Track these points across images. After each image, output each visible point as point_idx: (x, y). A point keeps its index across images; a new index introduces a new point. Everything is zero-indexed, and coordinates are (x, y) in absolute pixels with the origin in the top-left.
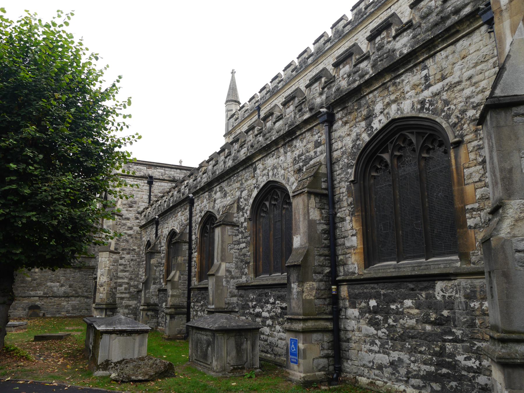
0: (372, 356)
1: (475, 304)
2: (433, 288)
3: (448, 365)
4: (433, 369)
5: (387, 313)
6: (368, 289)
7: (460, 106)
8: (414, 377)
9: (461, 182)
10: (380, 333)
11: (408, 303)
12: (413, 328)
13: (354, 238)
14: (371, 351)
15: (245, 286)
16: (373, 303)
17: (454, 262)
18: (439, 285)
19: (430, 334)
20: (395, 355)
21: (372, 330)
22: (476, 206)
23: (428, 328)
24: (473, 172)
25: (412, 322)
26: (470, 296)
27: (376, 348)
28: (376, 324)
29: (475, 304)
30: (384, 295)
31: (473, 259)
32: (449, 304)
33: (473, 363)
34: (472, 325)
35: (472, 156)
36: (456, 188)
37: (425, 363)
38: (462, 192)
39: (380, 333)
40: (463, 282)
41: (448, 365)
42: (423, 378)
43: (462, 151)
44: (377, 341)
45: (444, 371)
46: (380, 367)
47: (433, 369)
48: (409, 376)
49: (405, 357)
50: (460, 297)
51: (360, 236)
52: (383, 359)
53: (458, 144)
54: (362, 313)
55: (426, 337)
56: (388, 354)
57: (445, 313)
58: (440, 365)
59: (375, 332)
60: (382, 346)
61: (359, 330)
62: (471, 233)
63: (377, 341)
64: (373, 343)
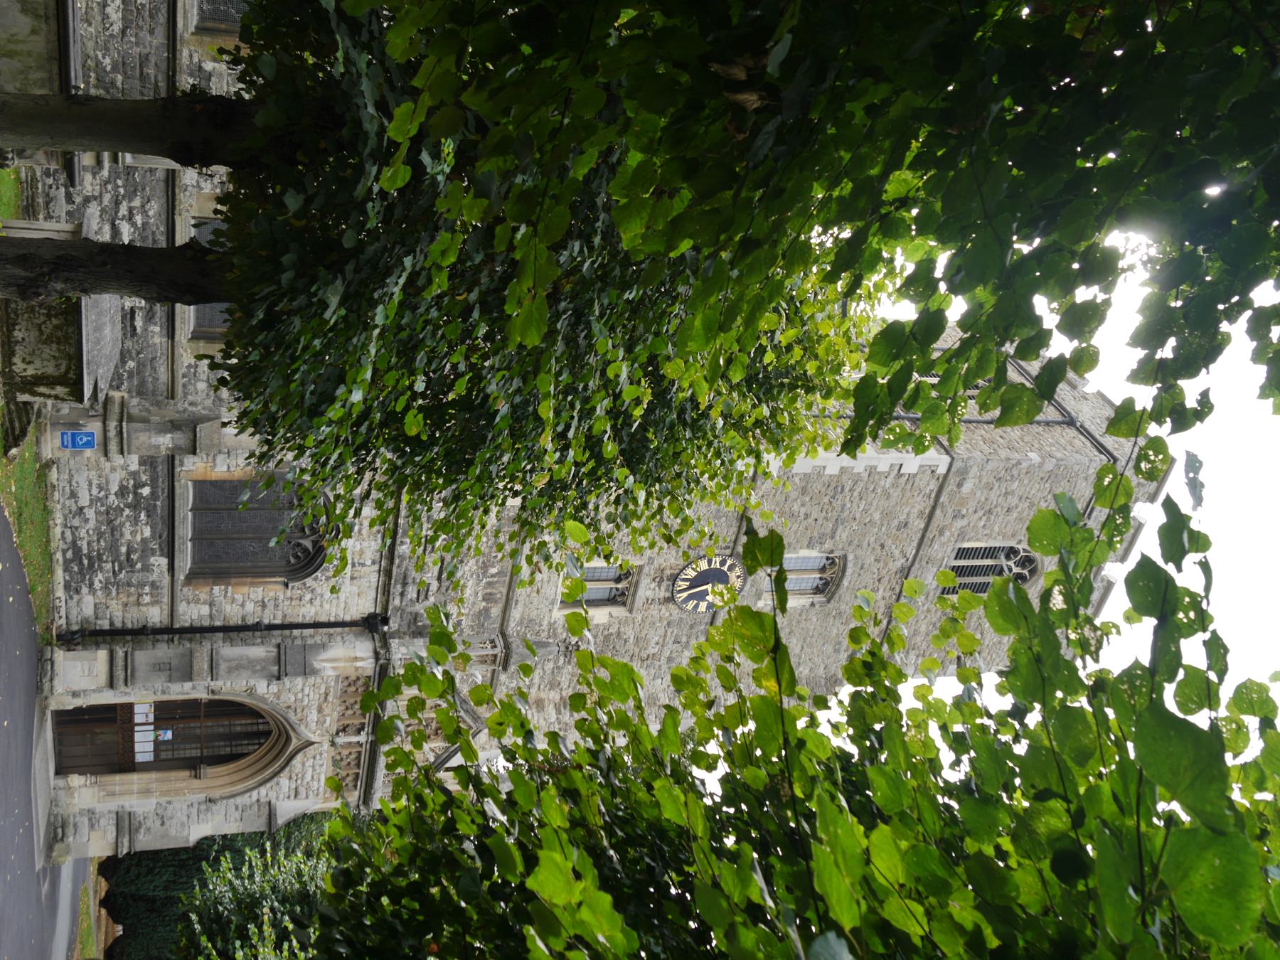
0: (85, 485)
1: (147, 589)
2: (161, 555)
3: (91, 565)
4: (85, 551)
5: (135, 506)
6: (162, 483)
7: (319, 590)
8: (73, 533)
9: (252, 584)
10: (112, 498)
11: (147, 532)
12: (122, 535)
13: (225, 468)
14: (90, 485)
15: (174, 208)
16: (146, 491)
17: (185, 561)
18: (164, 561)
19: (117, 550)
20: (90, 514)
21: (114, 488)
22: (229, 594)
23: (124, 549)
24: (258, 592)
25: (128, 536)
26: (153, 585)
27: (95, 491)
28: (122, 492)
29: (147, 589)
30: (155, 506)
31: (185, 589)
32: (147, 568)
33: (97, 585)
34: (129, 585)
35: (272, 594)
36: (249, 580)
37: (89, 544)
38: (244, 584)
39: (112, 498)
40: (166, 580)
41: (91, 565)
42: (74, 542)
43: (281, 587)
44: (103, 493)
45: (86, 562)
46: (73, 495)
47: (85, 551)
48: (74, 529)
49: (92, 524)
50: (154, 577)
51: (226, 476)
52: (84, 500)
53: (286, 585)
54: (134, 475)
55: (113, 547)
56: (90, 506)
57: (139, 566)
58: (90, 558)
59: (113, 492)
60: (99, 499)
61: (113, 469)
62: (208, 589)
63: (103, 493)
64: (100, 488)
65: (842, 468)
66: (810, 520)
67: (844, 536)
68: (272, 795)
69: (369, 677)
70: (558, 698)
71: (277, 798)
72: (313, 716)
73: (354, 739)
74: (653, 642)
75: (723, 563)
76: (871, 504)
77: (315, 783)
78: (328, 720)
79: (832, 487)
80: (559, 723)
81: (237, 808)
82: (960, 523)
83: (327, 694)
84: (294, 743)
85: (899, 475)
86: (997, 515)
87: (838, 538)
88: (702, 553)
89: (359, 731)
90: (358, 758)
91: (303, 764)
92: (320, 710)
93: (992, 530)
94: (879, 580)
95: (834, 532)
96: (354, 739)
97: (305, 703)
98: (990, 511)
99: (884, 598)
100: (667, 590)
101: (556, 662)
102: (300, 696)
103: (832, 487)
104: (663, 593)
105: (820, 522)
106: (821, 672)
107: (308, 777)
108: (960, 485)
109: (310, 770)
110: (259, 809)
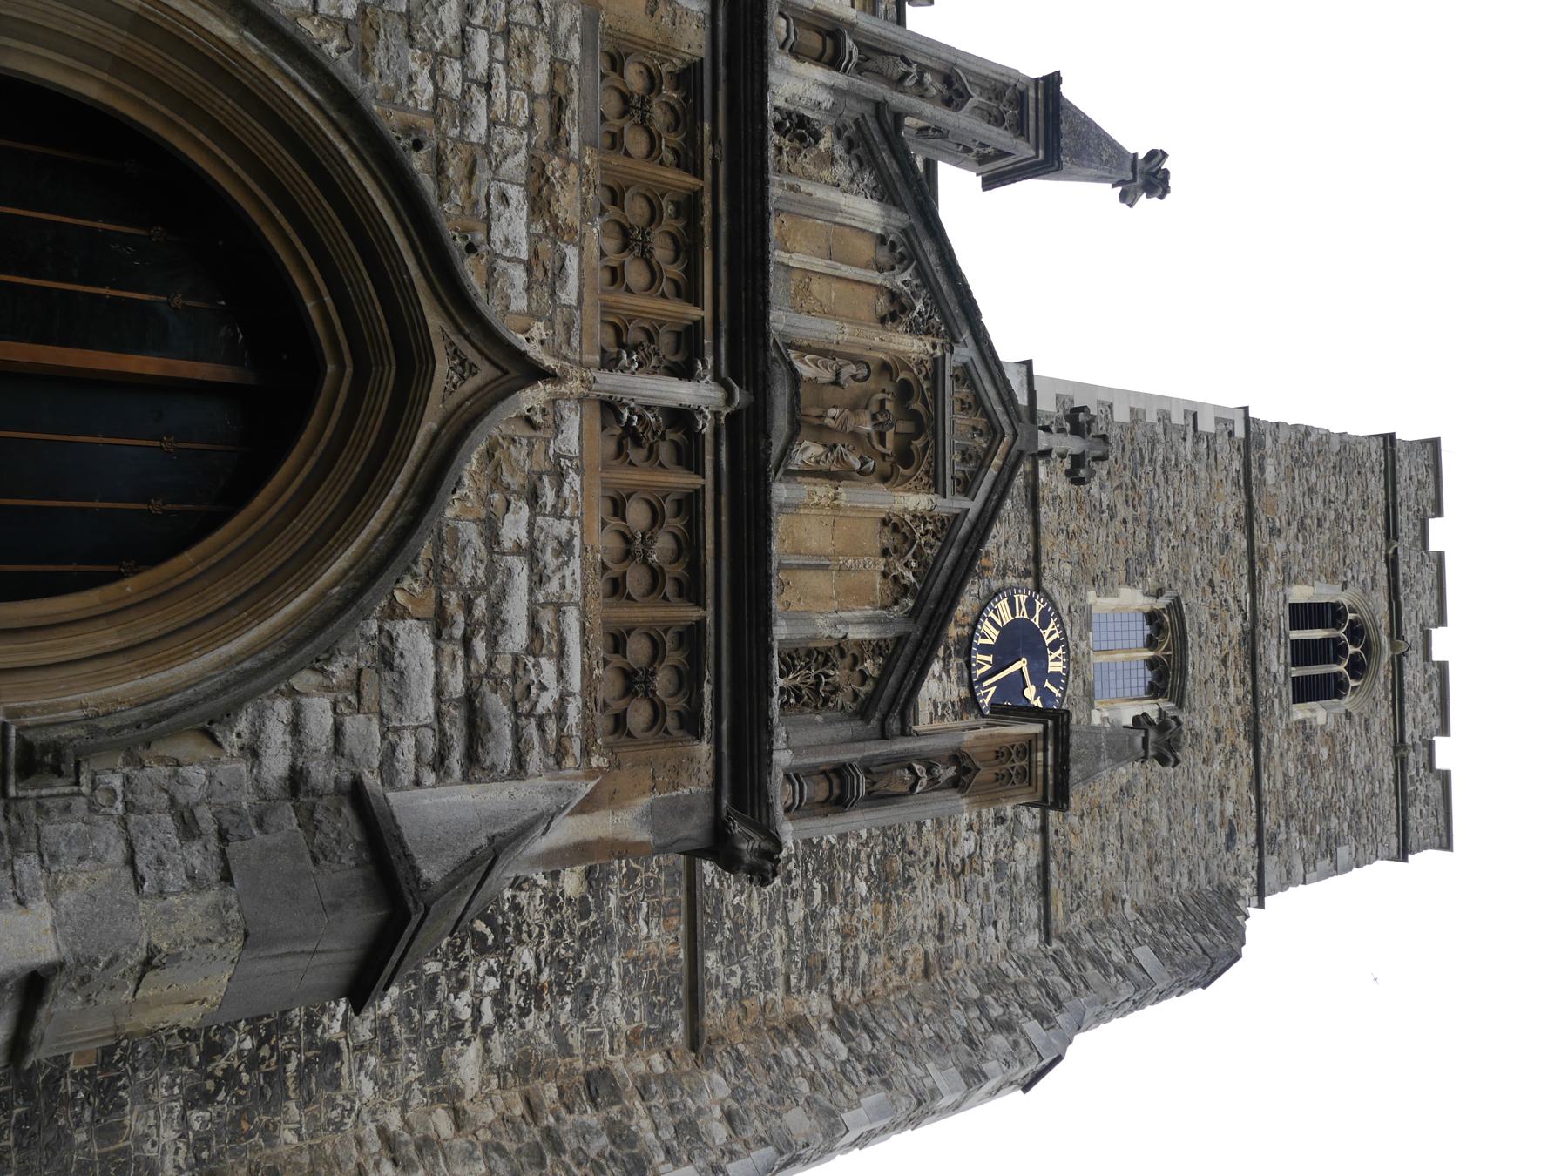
65: (1132, 410)
66: (1117, 522)
67: (1165, 557)
68: (363, 731)
69: (688, 77)
70: (828, 1008)
71: (387, 769)
72: (513, 227)
73: (681, 392)
74: (963, 823)
75: (1030, 604)
76: (1180, 493)
77: (548, 667)
78: (572, 253)
79: (1128, 454)
80: (859, 1059)
81: (188, 827)
82: (1280, 546)
83: (559, 105)
84: (446, 386)
85: (1197, 437)
86: (1312, 534)
87: (1159, 565)
88: (995, 585)
89: (685, 372)
90: (688, 546)
91: (492, 538)
92: (539, 204)
93: (1313, 563)
94: (1224, 661)
95: (1151, 546)
96: (681, 392)
97: (478, 130)
98: (1302, 524)
99: (1239, 702)
100: (960, 679)
101: (809, 895)
102: (453, 71)
103: (1128, 454)
104: (957, 692)
105: (1130, 525)
106: (1202, 879)
107: (517, 637)
108: (1262, 468)
109: (520, 568)
110: (309, 823)
